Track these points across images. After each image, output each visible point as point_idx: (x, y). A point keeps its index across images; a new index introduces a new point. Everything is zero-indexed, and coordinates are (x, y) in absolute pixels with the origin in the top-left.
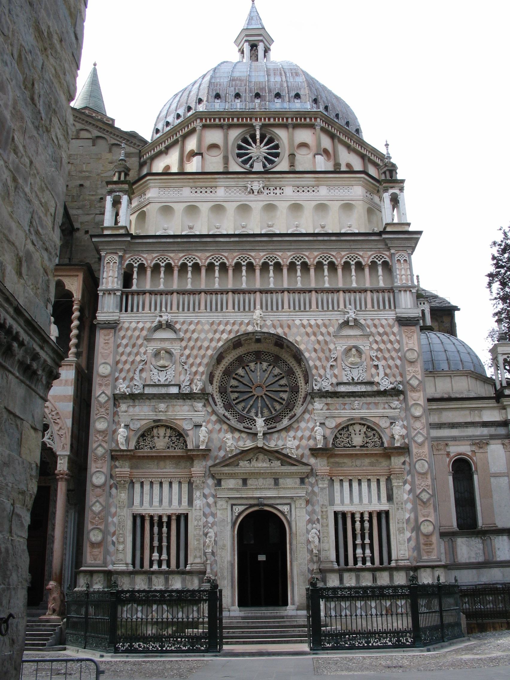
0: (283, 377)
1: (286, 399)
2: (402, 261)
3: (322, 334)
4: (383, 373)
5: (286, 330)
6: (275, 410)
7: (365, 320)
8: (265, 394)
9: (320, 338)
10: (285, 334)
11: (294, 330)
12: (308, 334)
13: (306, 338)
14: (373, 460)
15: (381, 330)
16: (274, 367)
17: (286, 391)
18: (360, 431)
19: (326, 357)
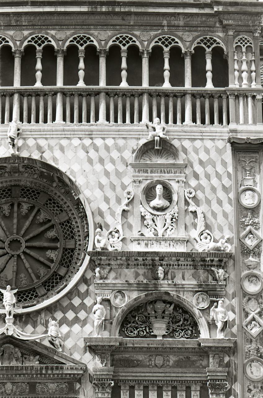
0: (52, 227)
1: (55, 259)
2: (244, 49)
3: (113, 161)
4: (203, 224)
5: (57, 153)
6: (38, 277)
7: (179, 139)
8: (24, 253)
9: (109, 167)
10: (55, 159)
11: (69, 154)
12: (90, 161)
13: (87, 166)
14: (181, 357)
15: (204, 156)
16: (39, 211)
17: (55, 249)
18: (164, 312)
19: (117, 197)
